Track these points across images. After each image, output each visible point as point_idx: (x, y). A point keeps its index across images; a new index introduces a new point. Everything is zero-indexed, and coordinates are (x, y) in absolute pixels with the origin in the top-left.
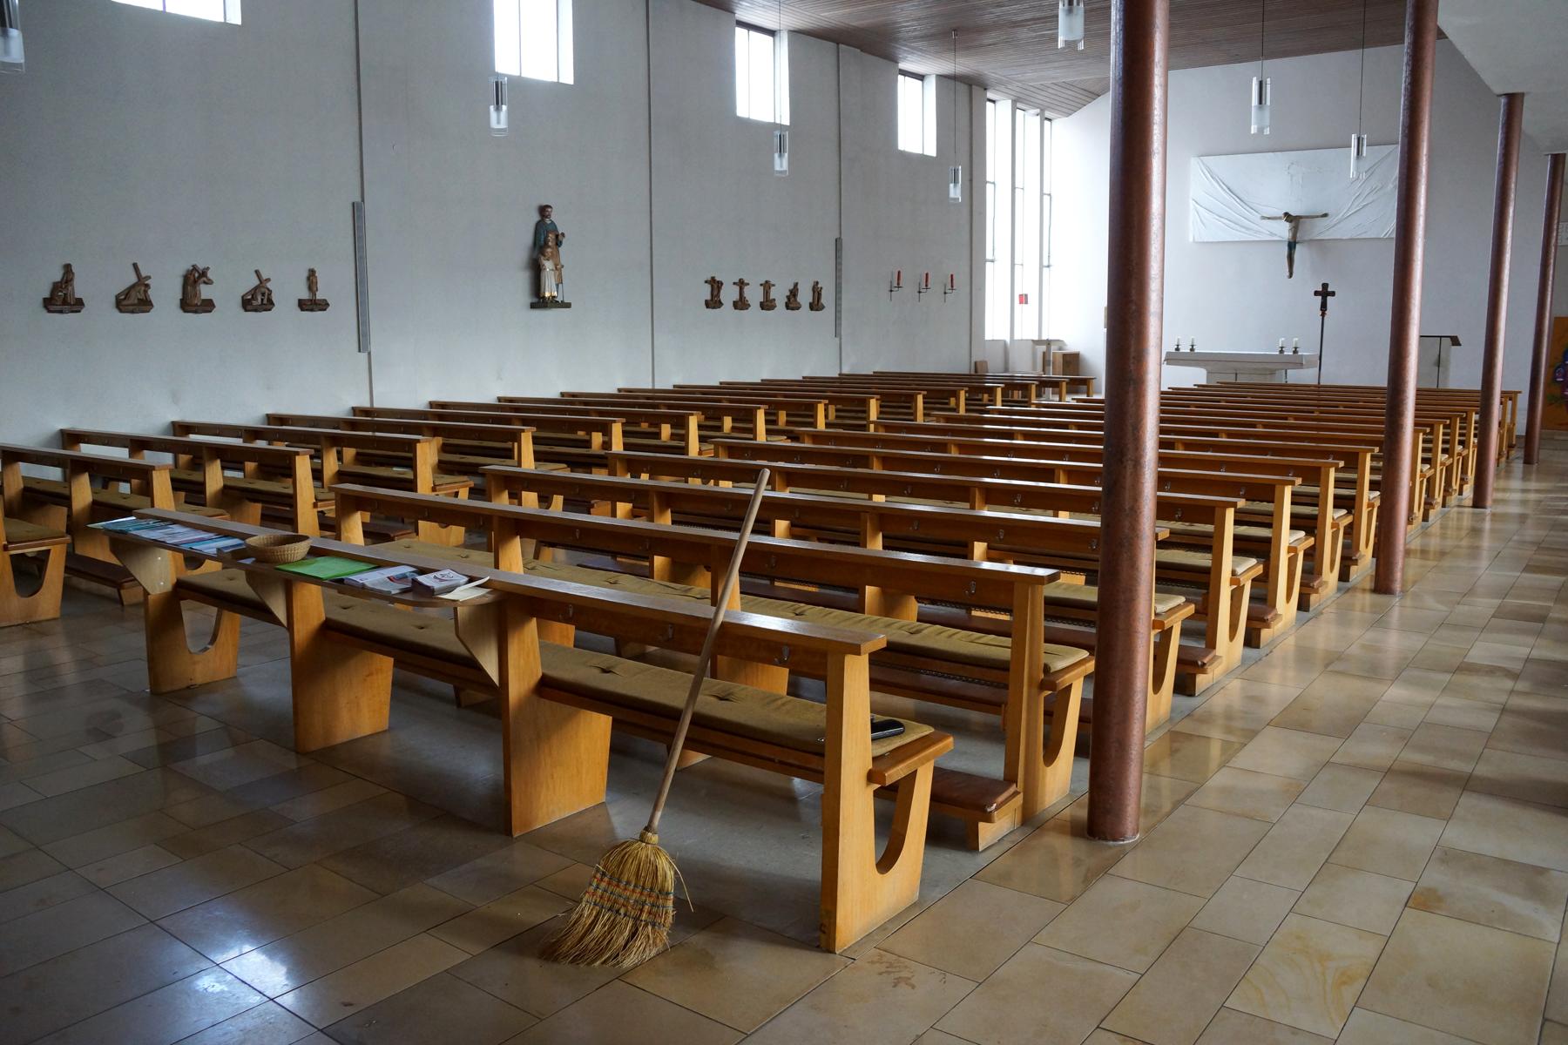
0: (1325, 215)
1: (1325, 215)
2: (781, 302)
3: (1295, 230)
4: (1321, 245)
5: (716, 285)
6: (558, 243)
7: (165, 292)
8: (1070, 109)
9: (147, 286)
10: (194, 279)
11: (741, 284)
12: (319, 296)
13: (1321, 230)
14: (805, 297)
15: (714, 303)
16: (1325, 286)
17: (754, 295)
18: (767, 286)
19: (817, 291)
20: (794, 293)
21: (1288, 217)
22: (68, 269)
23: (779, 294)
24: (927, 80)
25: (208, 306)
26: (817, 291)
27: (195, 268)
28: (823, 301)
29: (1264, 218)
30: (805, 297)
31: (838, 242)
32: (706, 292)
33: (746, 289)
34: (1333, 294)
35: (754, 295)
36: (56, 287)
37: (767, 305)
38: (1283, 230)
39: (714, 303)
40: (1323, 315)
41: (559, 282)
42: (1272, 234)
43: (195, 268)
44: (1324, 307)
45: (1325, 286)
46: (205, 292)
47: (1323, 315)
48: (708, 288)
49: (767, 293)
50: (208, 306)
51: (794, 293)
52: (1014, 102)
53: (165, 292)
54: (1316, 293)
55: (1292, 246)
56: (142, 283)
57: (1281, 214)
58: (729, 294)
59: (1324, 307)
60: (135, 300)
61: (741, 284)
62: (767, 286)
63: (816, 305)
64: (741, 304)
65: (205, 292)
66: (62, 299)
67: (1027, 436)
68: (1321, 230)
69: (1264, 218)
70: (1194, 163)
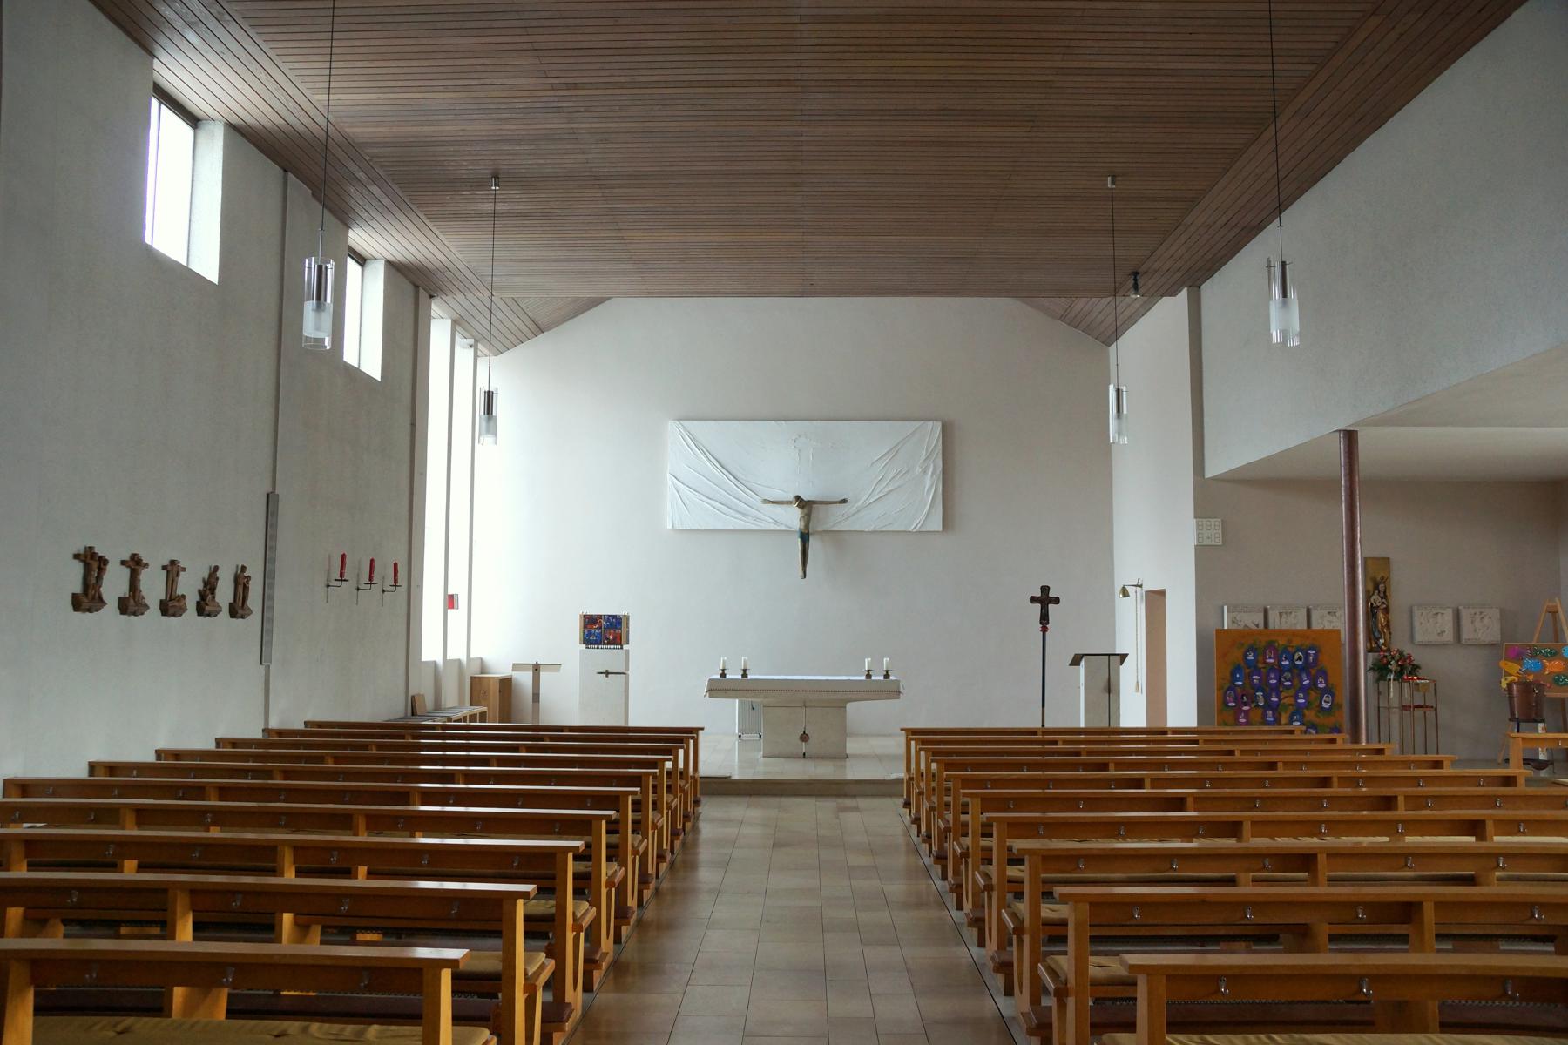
0: (844, 501)
1: (844, 501)
2: (192, 601)
3: (807, 518)
4: (837, 538)
5: (93, 563)
11: (135, 564)
13: (836, 519)
15: (87, 599)
16: (1045, 589)
17: (153, 587)
19: (241, 582)
20: (210, 586)
23: (189, 586)
24: (370, 267)
26: (241, 582)
28: (250, 603)
29: (766, 501)
31: (271, 499)
34: (1056, 601)
35: (153, 587)
38: (792, 518)
39: (87, 599)
40: (1044, 630)
44: (1044, 618)
45: (1045, 589)
47: (1044, 630)
48: (78, 569)
49: (171, 582)
51: (210, 586)
52: (454, 322)
54: (1033, 600)
55: (805, 537)
57: (791, 497)
58: (114, 584)
59: (1044, 618)
61: (135, 564)
64: (131, 605)
67: (287, 774)
68: (836, 519)
69: (766, 501)
70: (673, 429)
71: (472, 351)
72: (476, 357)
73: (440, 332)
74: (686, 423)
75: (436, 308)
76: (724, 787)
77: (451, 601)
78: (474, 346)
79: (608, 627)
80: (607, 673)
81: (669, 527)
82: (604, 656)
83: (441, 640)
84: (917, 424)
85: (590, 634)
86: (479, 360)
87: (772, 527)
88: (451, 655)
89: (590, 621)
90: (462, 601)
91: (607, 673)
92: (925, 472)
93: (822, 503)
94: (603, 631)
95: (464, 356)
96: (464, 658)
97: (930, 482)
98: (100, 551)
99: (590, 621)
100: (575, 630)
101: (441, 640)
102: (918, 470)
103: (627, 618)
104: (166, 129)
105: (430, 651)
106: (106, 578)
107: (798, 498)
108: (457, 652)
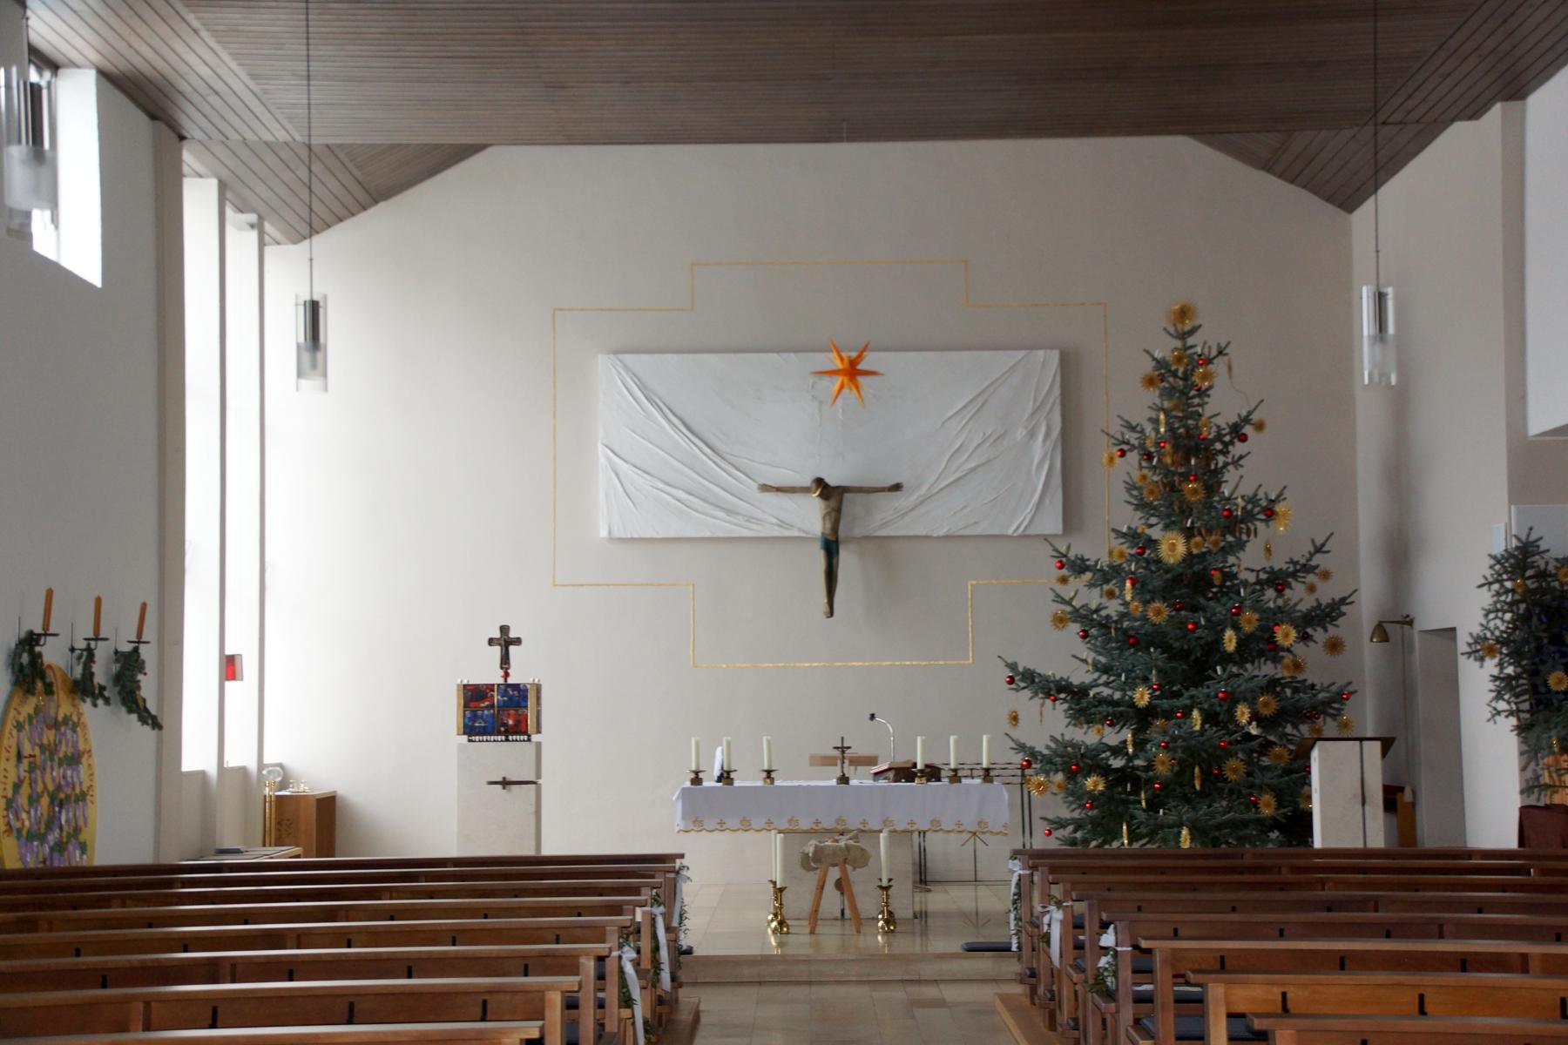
0: (897, 487)
1: (897, 487)
3: (835, 516)
8: (310, 226)
13: (886, 518)
21: (824, 488)
29: (765, 488)
38: (810, 516)
42: (782, 524)
52: (223, 187)
55: (831, 548)
57: (807, 481)
69: (765, 488)
71: (253, 236)
72: (262, 245)
73: (199, 202)
74: (627, 358)
75: (188, 157)
76: (732, 972)
77: (230, 667)
78: (258, 226)
79: (504, 706)
80: (505, 783)
81: (604, 533)
82: (499, 754)
83: (215, 732)
84: (1021, 354)
85: (475, 717)
86: (268, 250)
87: (777, 532)
88: (232, 761)
89: (474, 695)
90: (249, 667)
91: (505, 783)
92: (1032, 434)
93: (860, 490)
94: (497, 712)
95: (243, 242)
97: (1041, 454)
99: (474, 695)
100: (450, 711)
101: (215, 732)
102: (1021, 433)
103: (538, 688)
105: (197, 754)
107: (820, 482)
108: (240, 755)
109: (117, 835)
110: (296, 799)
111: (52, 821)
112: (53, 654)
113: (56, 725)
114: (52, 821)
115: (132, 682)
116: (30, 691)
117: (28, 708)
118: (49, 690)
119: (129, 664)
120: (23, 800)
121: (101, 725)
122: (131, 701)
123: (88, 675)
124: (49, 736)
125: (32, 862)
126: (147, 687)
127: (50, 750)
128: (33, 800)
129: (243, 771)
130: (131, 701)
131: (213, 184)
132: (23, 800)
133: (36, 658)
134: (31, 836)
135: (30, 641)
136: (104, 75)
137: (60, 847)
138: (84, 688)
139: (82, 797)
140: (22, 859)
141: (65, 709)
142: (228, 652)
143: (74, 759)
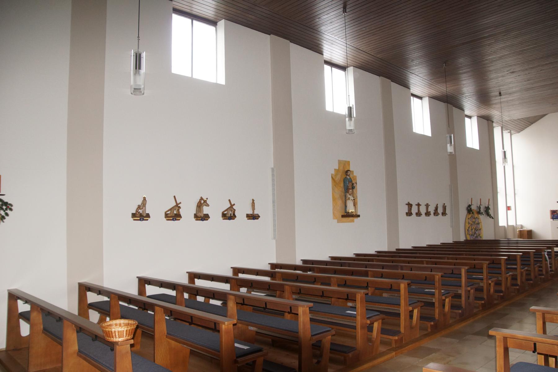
2: (432, 213)
5: (410, 205)
6: (353, 188)
7: (188, 211)
9: (180, 207)
10: (202, 203)
11: (419, 205)
12: (255, 213)
14: (440, 211)
15: (409, 214)
17: (423, 210)
18: (427, 206)
19: (444, 208)
20: (436, 209)
22: (145, 199)
23: (431, 209)
24: (472, 119)
25: (206, 217)
26: (444, 208)
27: (202, 199)
28: (447, 212)
30: (440, 211)
32: (406, 209)
33: (421, 207)
35: (423, 210)
36: (139, 207)
37: (428, 214)
39: (409, 214)
41: (355, 204)
43: (202, 199)
46: (206, 210)
48: (407, 206)
50: (206, 217)
51: (436, 209)
53: (188, 211)
56: (178, 206)
58: (414, 210)
60: (174, 215)
61: (419, 205)
62: (427, 206)
63: (444, 214)
64: (419, 214)
65: (206, 210)
66: (140, 215)
71: (509, 134)
72: (511, 135)
73: (497, 132)
75: (494, 124)
77: (509, 208)
78: (510, 132)
83: (504, 219)
86: (513, 136)
88: (510, 224)
90: (513, 208)
95: (507, 135)
96: (515, 225)
98: (411, 203)
100: (549, 215)
101: (504, 219)
104: (415, 102)
105: (502, 222)
106: (412, 208)
108: (512, 223)
109: (487, 234)
110: (523, 231)
111: (475, 233)
112: (474, 207)
113: (475, 218)
114: (475, 233)
115: (489, 211)
116: (470, 213)
117: (470, 216)
118: (473, 213)
119: (487, 209)
120: (470, 229)
121: (483, 218)
122: (488, 214)
123: (480, 210)
124: (474, 220)
125: (472, 239)
126: (491, 212)
127: (474, 222)
128: (472, 230)
129: (513, 226)
130: (488, 214)
131: (500, 128)
132: (470, 229)
133: (471, 209)
134: (472, 235)
135: (469, 206)
136: (478, 116)
137: (477, 237)
138: (479, 213)
139: (480, 229)
140: (466, 237)
141: (476, 216)
142: (508, 205)
143: (478, 224)
